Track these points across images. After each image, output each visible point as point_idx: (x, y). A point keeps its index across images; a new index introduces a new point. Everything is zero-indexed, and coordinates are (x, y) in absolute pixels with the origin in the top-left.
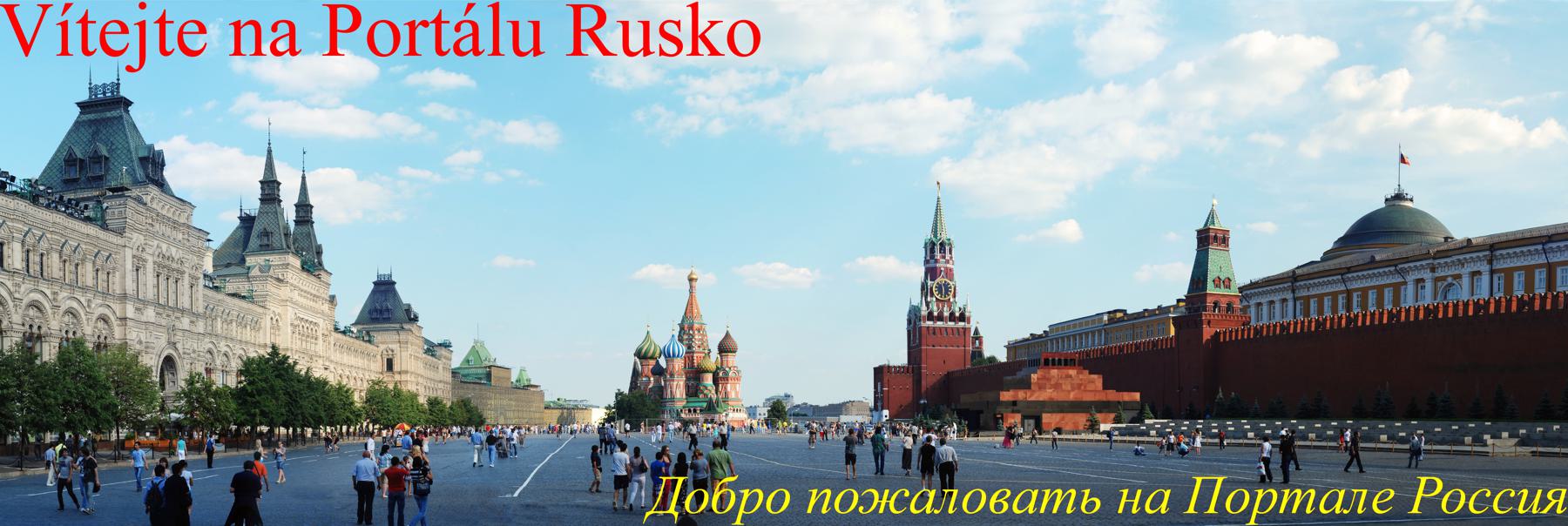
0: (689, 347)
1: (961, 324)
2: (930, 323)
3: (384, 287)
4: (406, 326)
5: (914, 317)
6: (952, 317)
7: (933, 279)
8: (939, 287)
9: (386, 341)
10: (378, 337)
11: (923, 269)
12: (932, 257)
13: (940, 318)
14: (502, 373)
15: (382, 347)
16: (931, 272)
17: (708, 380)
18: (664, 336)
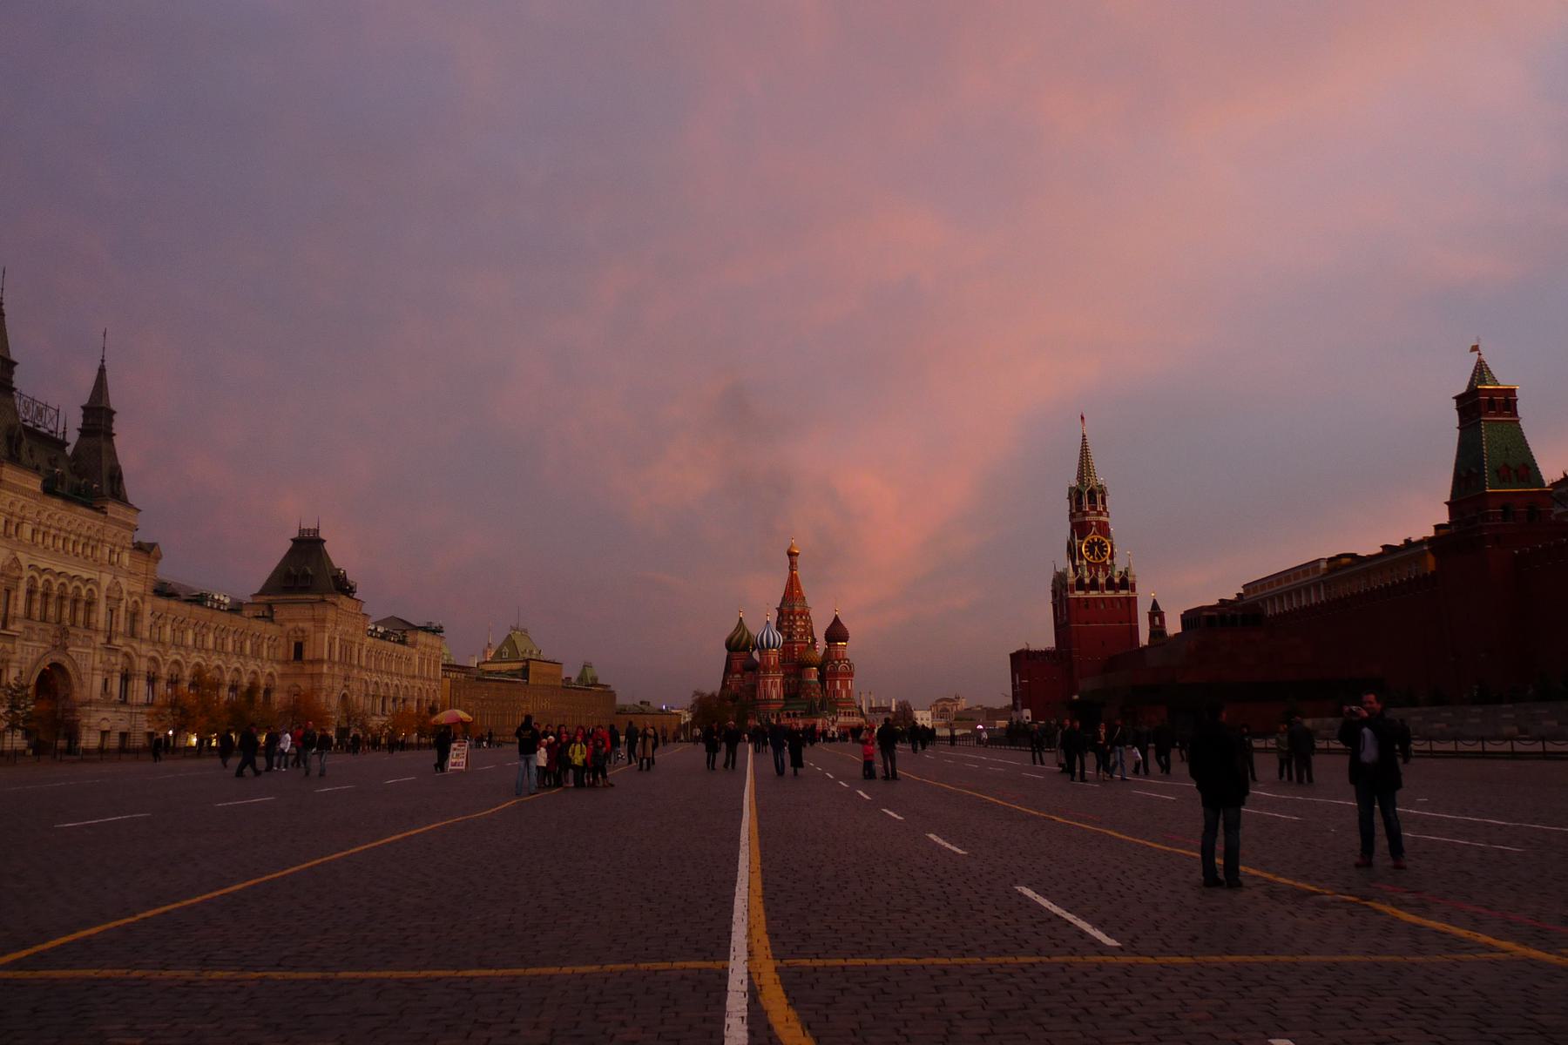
0: (790, 636)
1: (1123, 593)
2: (1080, 594)
3: (308, 547)
4: (329, 598)
5: (1060, 586)
6: (1110, 584)
7: (1081, 538)
8: (1090, 548)
9: (295, 616)
10: (281, 613)
11: (1069, 525)
12: (1079, 508)
13: (1094, 585)
14: (546, 668)
15: (290, 626)
16: (1079, 528)
17: (813, 675)
18: (762, 623)
